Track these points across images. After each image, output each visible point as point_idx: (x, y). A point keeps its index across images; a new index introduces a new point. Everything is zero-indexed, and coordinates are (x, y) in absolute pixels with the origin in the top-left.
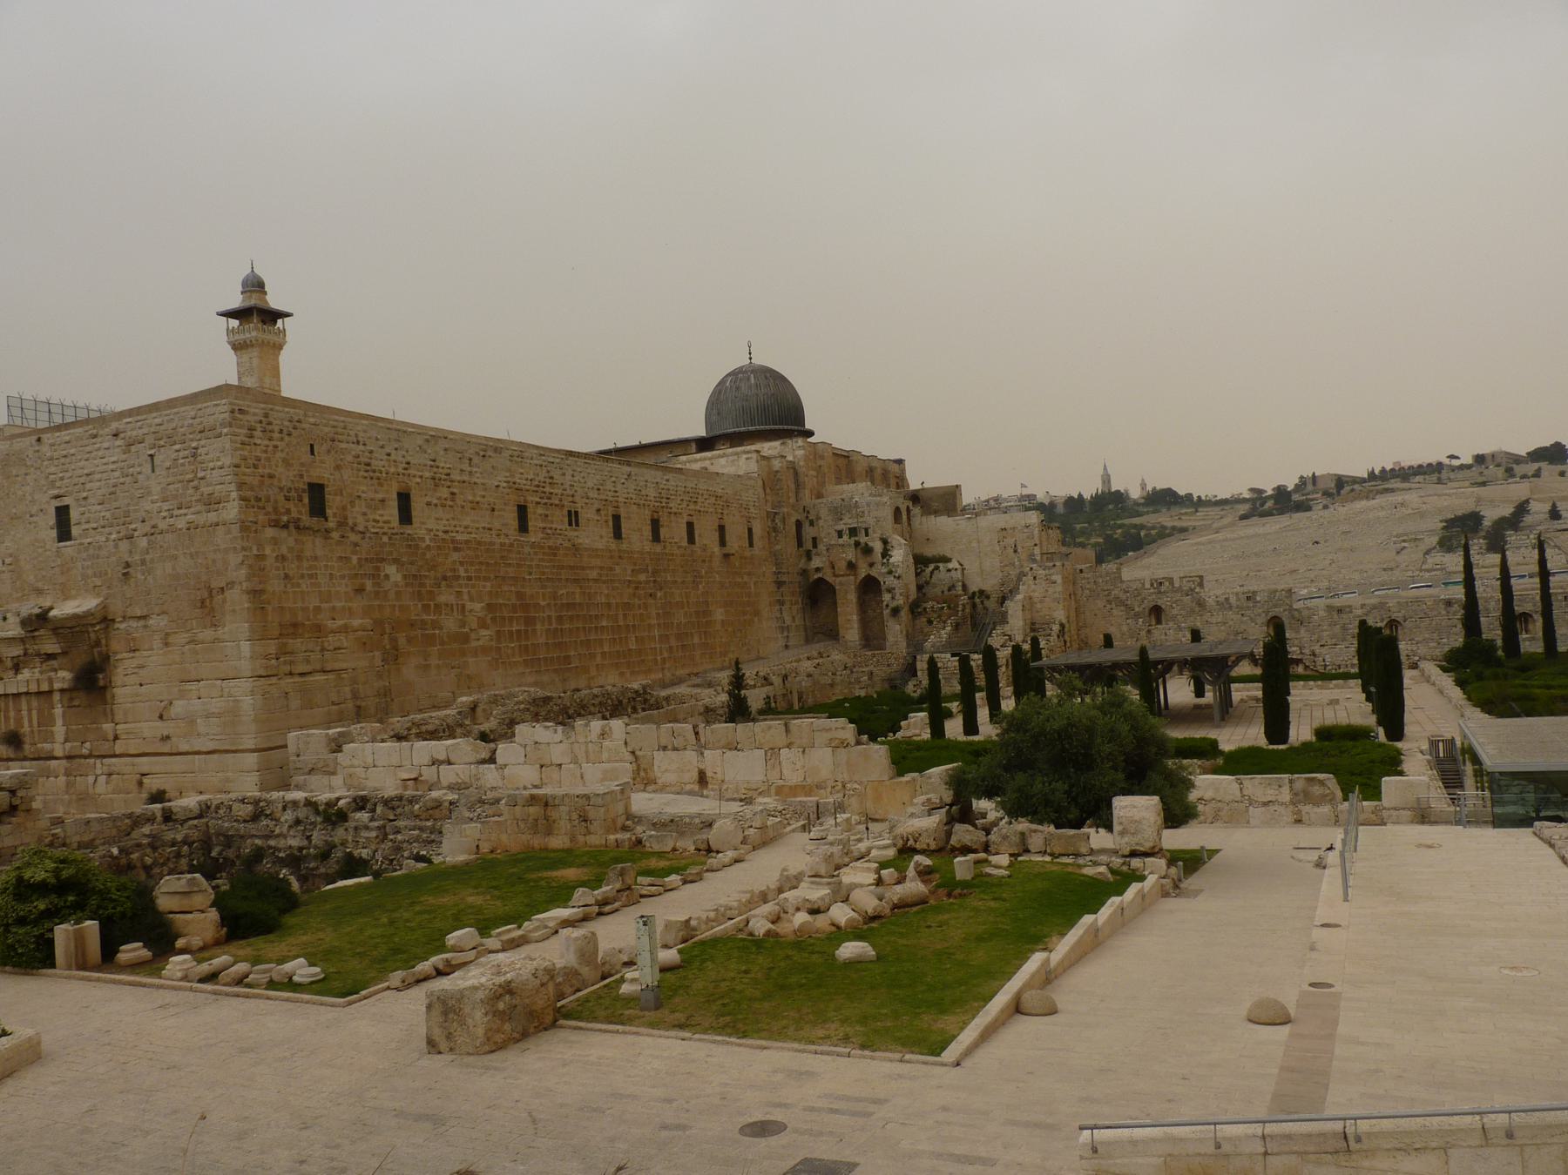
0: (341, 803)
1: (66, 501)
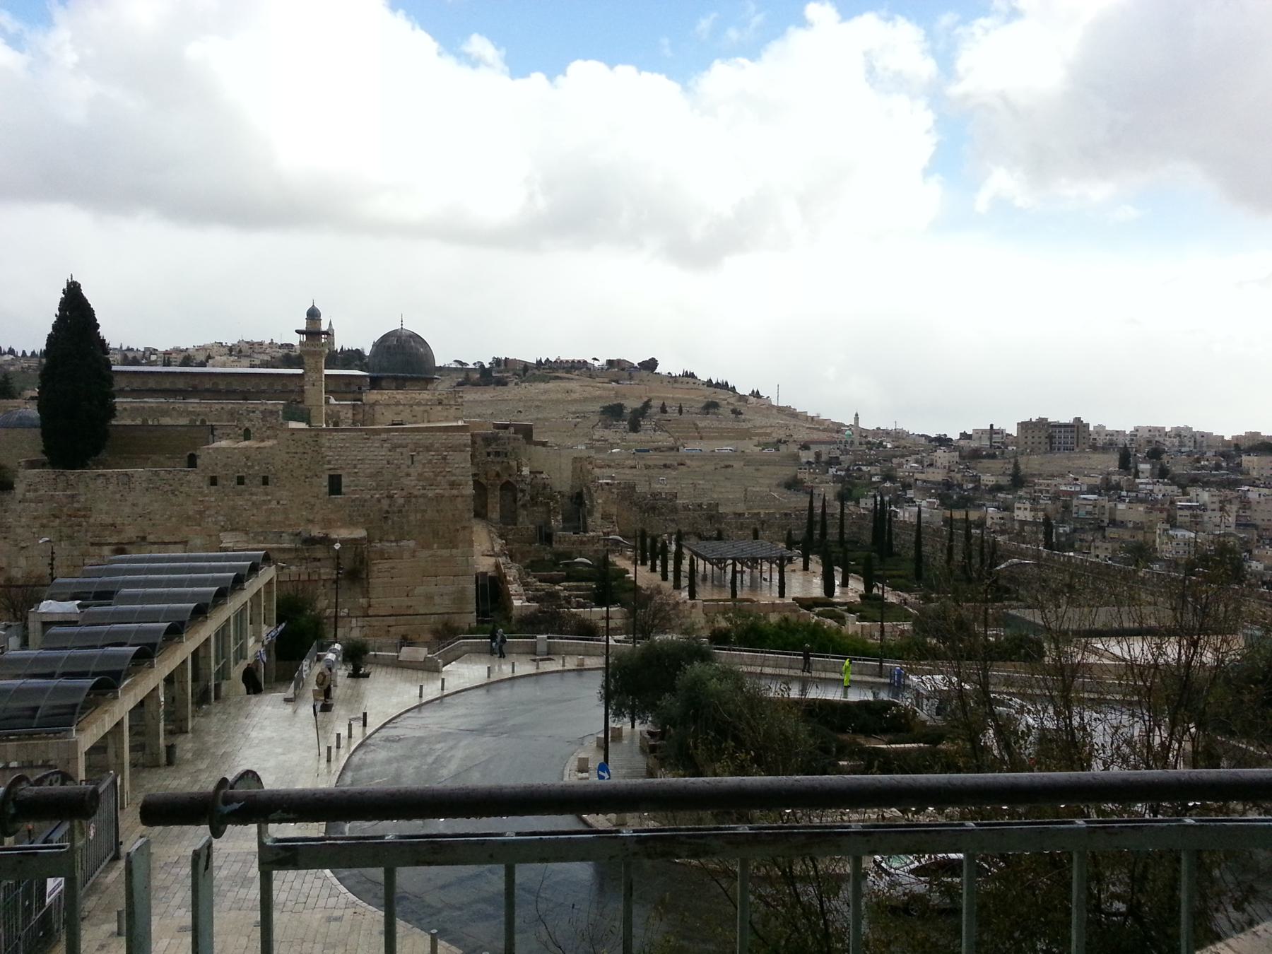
1: (339, 472)
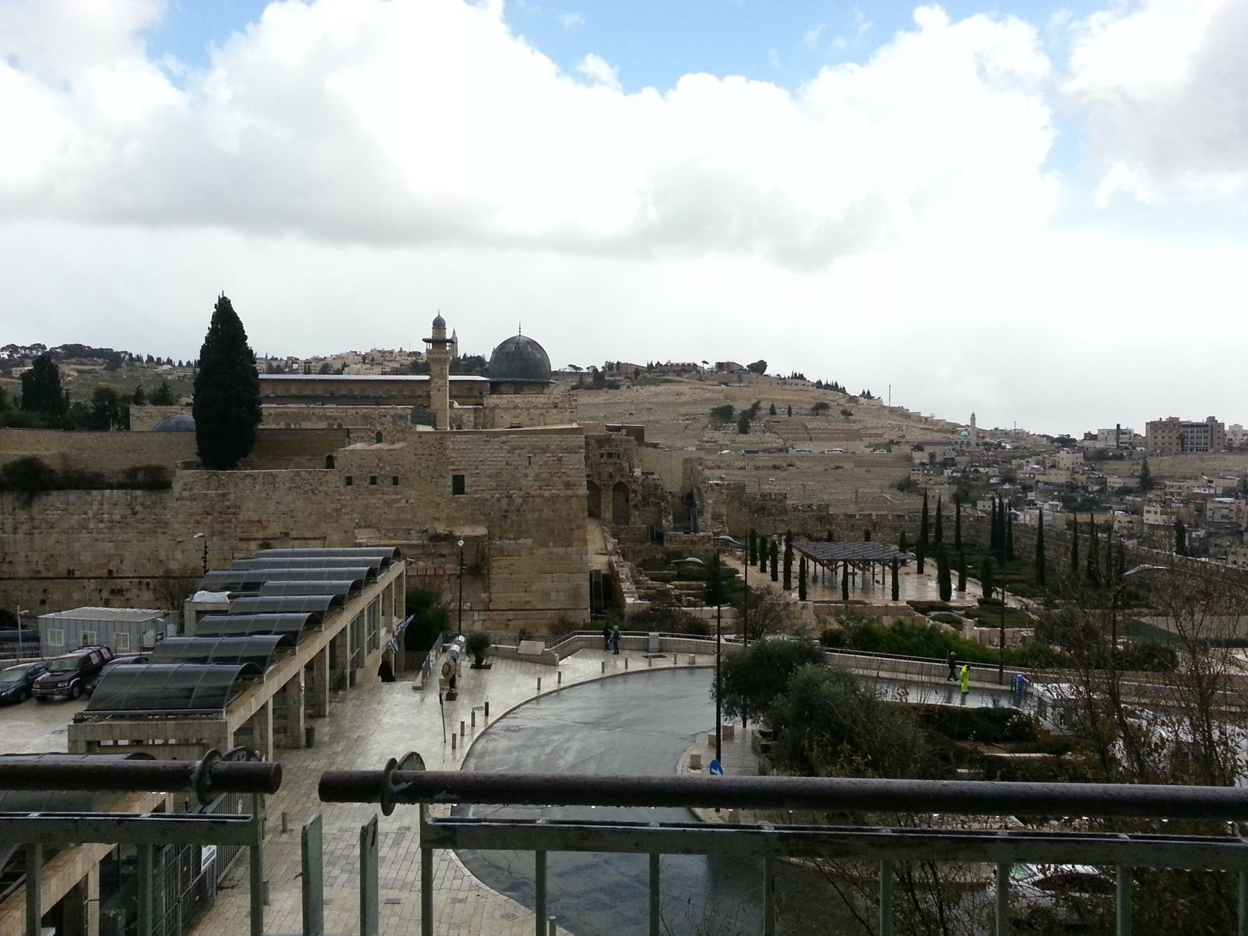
1: (462, 473)
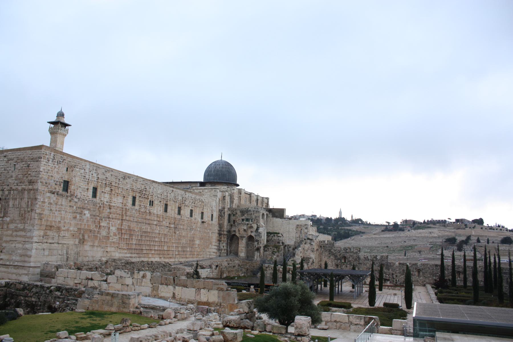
0: (52, 288)
